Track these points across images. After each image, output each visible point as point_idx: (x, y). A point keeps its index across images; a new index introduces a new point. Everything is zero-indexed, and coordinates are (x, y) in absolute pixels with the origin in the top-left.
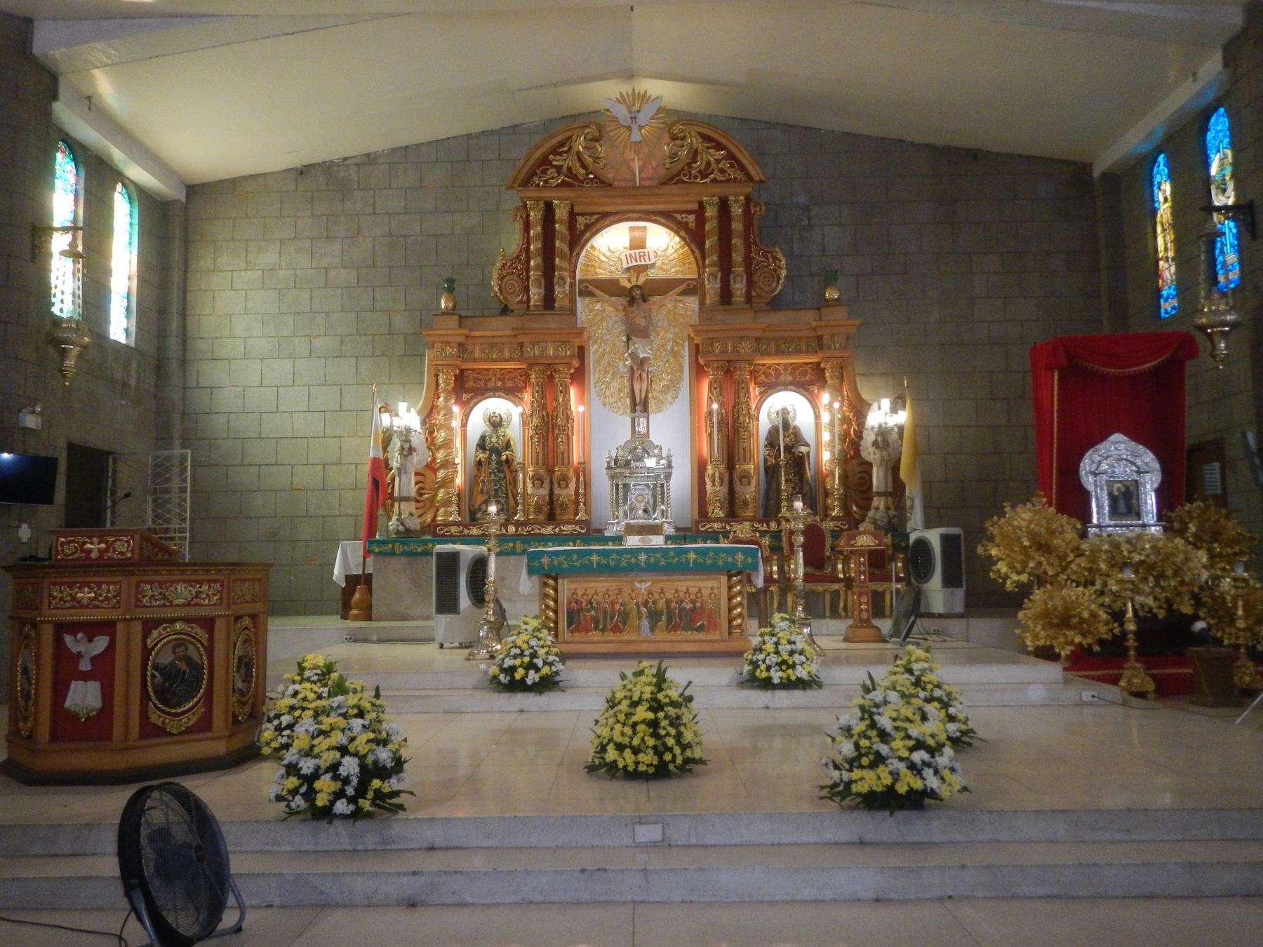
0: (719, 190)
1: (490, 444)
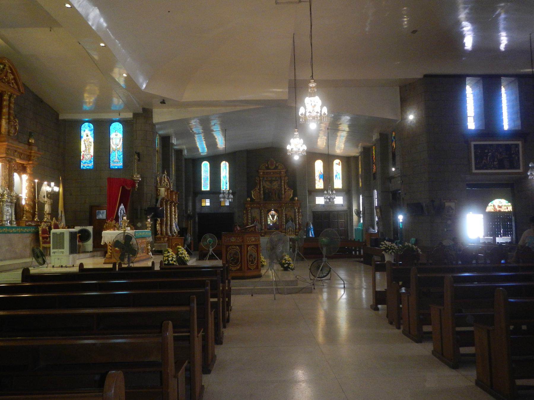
0: (12, 90)
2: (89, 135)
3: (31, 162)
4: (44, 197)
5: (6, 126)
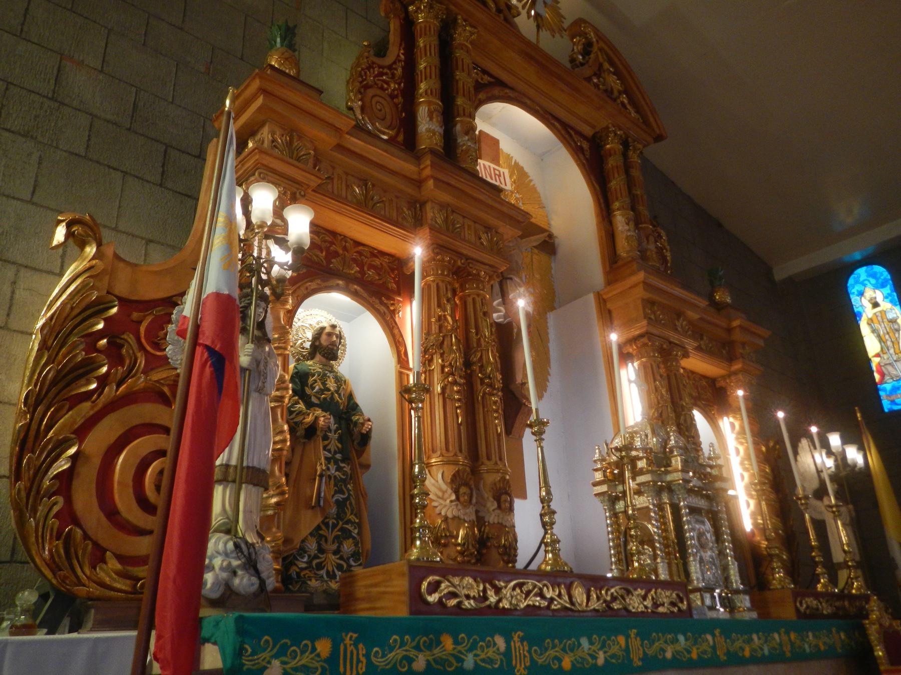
1: (321, 391)
2: (880, 299)
3: (737, 366)
4: (820, 493)
5: (629, 230)
